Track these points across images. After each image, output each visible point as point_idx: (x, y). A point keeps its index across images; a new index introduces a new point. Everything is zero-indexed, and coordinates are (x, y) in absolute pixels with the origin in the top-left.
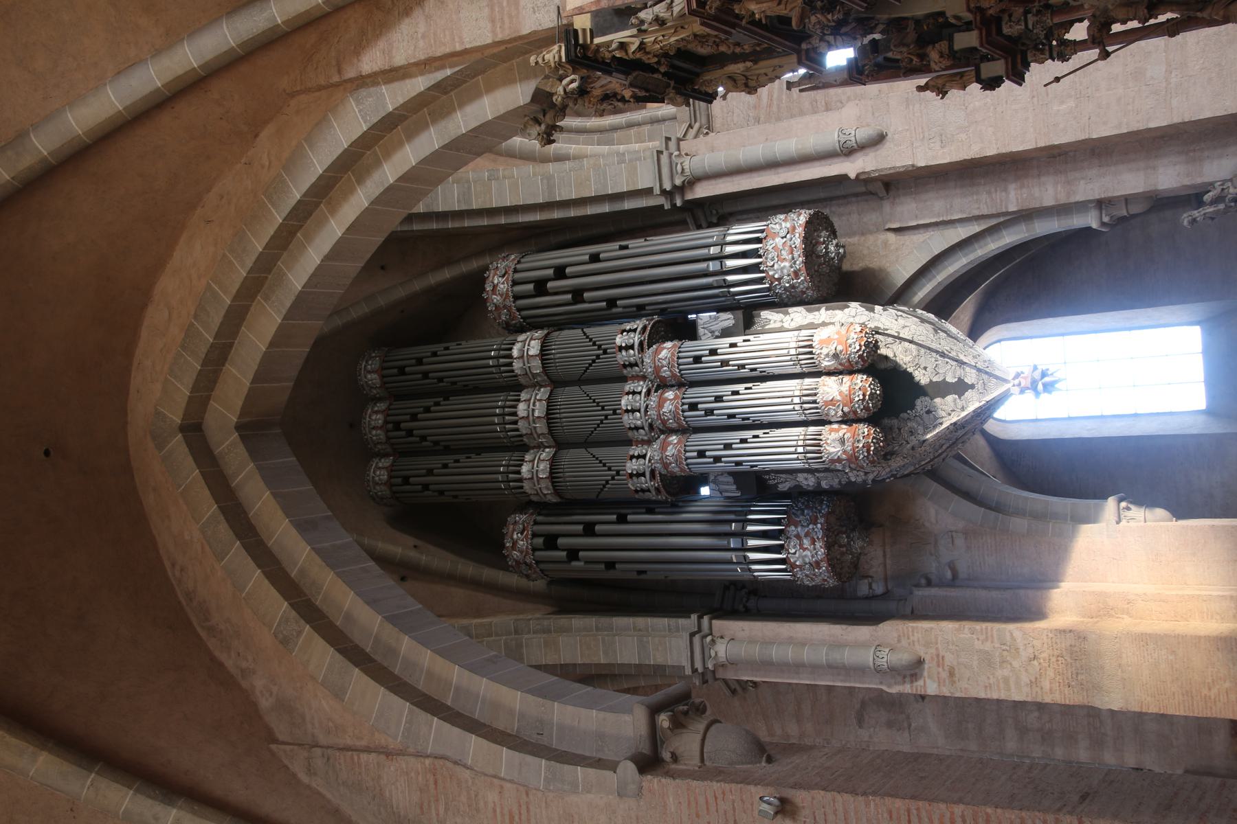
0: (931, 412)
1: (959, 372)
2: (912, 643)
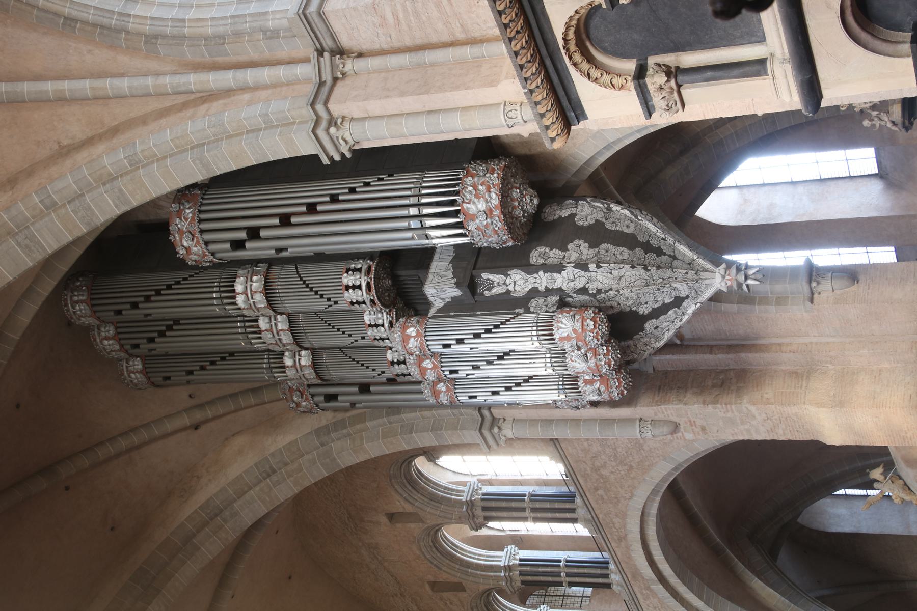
0: (658, 327)
1: (674, 293)
2: (667, 416)
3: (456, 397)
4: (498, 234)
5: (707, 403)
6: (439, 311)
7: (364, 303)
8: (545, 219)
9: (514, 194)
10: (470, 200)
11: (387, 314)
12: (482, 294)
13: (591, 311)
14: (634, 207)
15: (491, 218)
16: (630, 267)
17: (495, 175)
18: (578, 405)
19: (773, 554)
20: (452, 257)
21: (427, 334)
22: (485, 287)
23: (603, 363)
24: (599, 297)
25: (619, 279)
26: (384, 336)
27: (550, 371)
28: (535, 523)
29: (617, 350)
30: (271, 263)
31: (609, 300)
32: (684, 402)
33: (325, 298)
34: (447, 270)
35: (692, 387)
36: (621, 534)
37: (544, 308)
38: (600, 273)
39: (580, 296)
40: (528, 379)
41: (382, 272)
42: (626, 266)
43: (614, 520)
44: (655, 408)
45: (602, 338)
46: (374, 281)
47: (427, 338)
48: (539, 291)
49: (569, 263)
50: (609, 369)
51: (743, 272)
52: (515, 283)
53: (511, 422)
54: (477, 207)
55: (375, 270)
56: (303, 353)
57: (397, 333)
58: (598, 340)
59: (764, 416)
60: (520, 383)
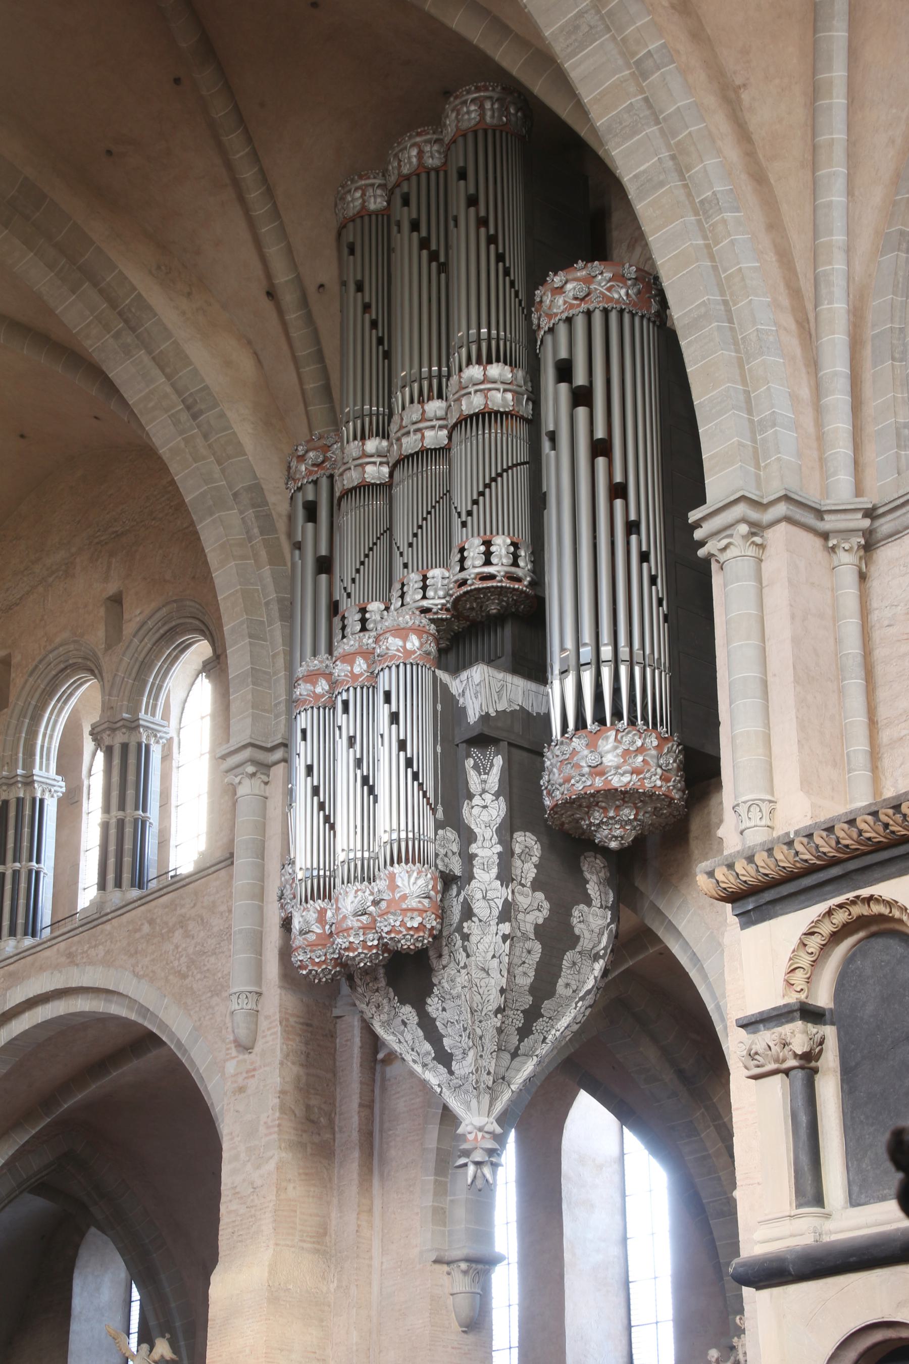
0: (405, 1026)
1: (457, 1053)
3: (305, 709)
4: (564, 783)
5: (282, 1096)
6: (445, 688)
7: (462, 569)
8: (585, 858)
9: (626, 811)
10: (620, 742)
11: (443, 605)
12: (469, 755)
13: (434, 923)
14: (598, 995)
15: (591, 774)
16: (502, 987)
17: (659, 783)
18: (285, 899)
19: (41, 1188)
20: (530, 710)
21: (408, 667)
22: (480, 760)
23: (351, 939)
24: (456, 937)
25: (483, 969)
26: (408, 599)
27: (341, 857)
28: (99, 825)
29: (371, 962)
30: (534, 423)
31: (452, 952)
32: (285, 1061)
33: (472, 508)
34: (510, 701)
35: (308, 1074)
36: (79, 958)
37: (442, 852)
38: (494, 940)
39: (460, 908)
40: (329, 823)
41: (511, 600)
42: (504, 980)
43: (101, 947)
44: (277, 1017)
45: (391, 939)
46: (497, 587)
47: (402, 667)
48: (470, 843)
49: (513, 892)
50: (341, 948)
51: (487, 1159)
52: (485, 807)
53: (263, 794)
54: (608, 752)
55: (514, 589)
56: (385, 470)
57: (411, 619)
58: (387, 933)
59: (258, 1182)
60: (324, 810)
